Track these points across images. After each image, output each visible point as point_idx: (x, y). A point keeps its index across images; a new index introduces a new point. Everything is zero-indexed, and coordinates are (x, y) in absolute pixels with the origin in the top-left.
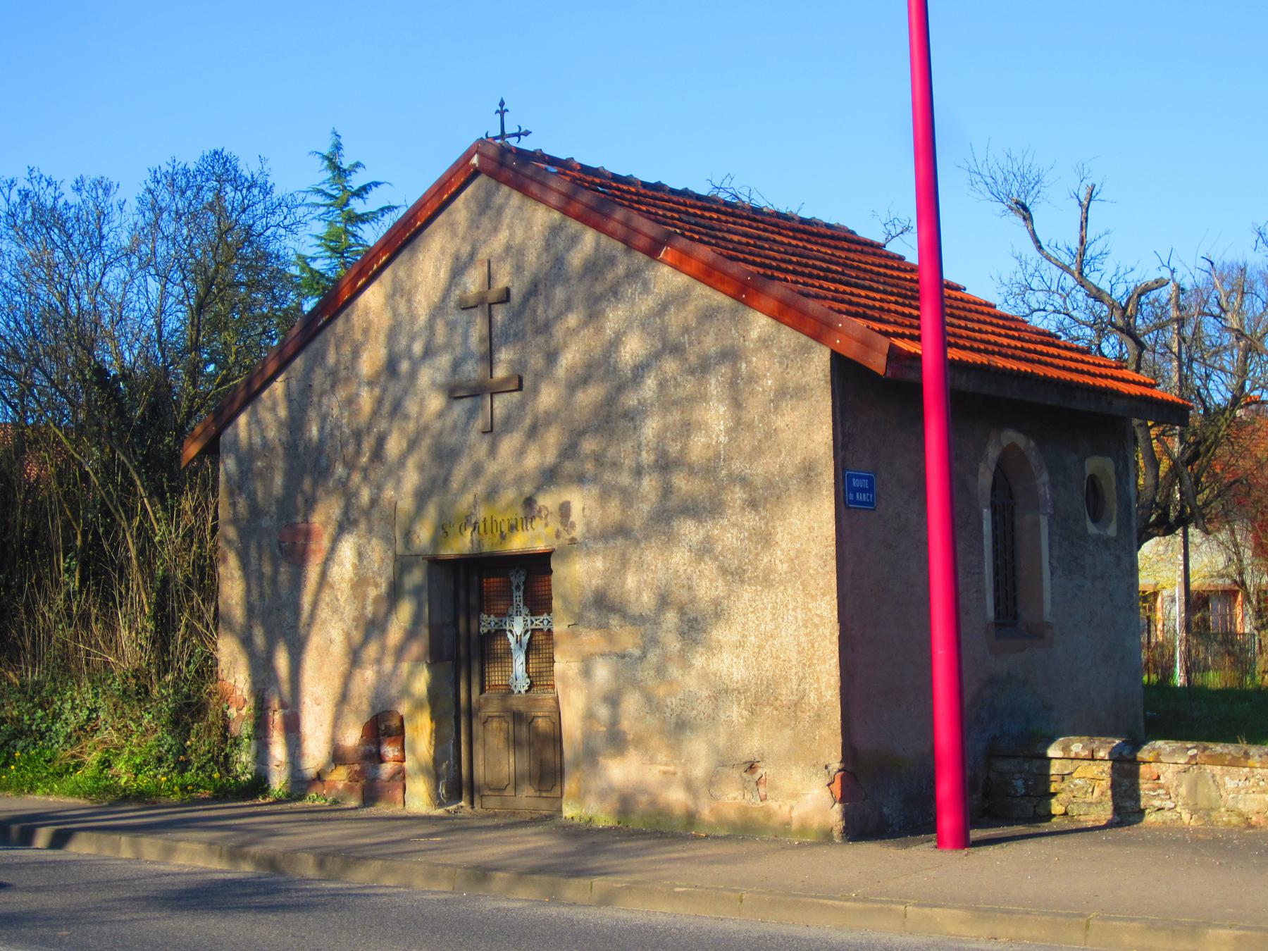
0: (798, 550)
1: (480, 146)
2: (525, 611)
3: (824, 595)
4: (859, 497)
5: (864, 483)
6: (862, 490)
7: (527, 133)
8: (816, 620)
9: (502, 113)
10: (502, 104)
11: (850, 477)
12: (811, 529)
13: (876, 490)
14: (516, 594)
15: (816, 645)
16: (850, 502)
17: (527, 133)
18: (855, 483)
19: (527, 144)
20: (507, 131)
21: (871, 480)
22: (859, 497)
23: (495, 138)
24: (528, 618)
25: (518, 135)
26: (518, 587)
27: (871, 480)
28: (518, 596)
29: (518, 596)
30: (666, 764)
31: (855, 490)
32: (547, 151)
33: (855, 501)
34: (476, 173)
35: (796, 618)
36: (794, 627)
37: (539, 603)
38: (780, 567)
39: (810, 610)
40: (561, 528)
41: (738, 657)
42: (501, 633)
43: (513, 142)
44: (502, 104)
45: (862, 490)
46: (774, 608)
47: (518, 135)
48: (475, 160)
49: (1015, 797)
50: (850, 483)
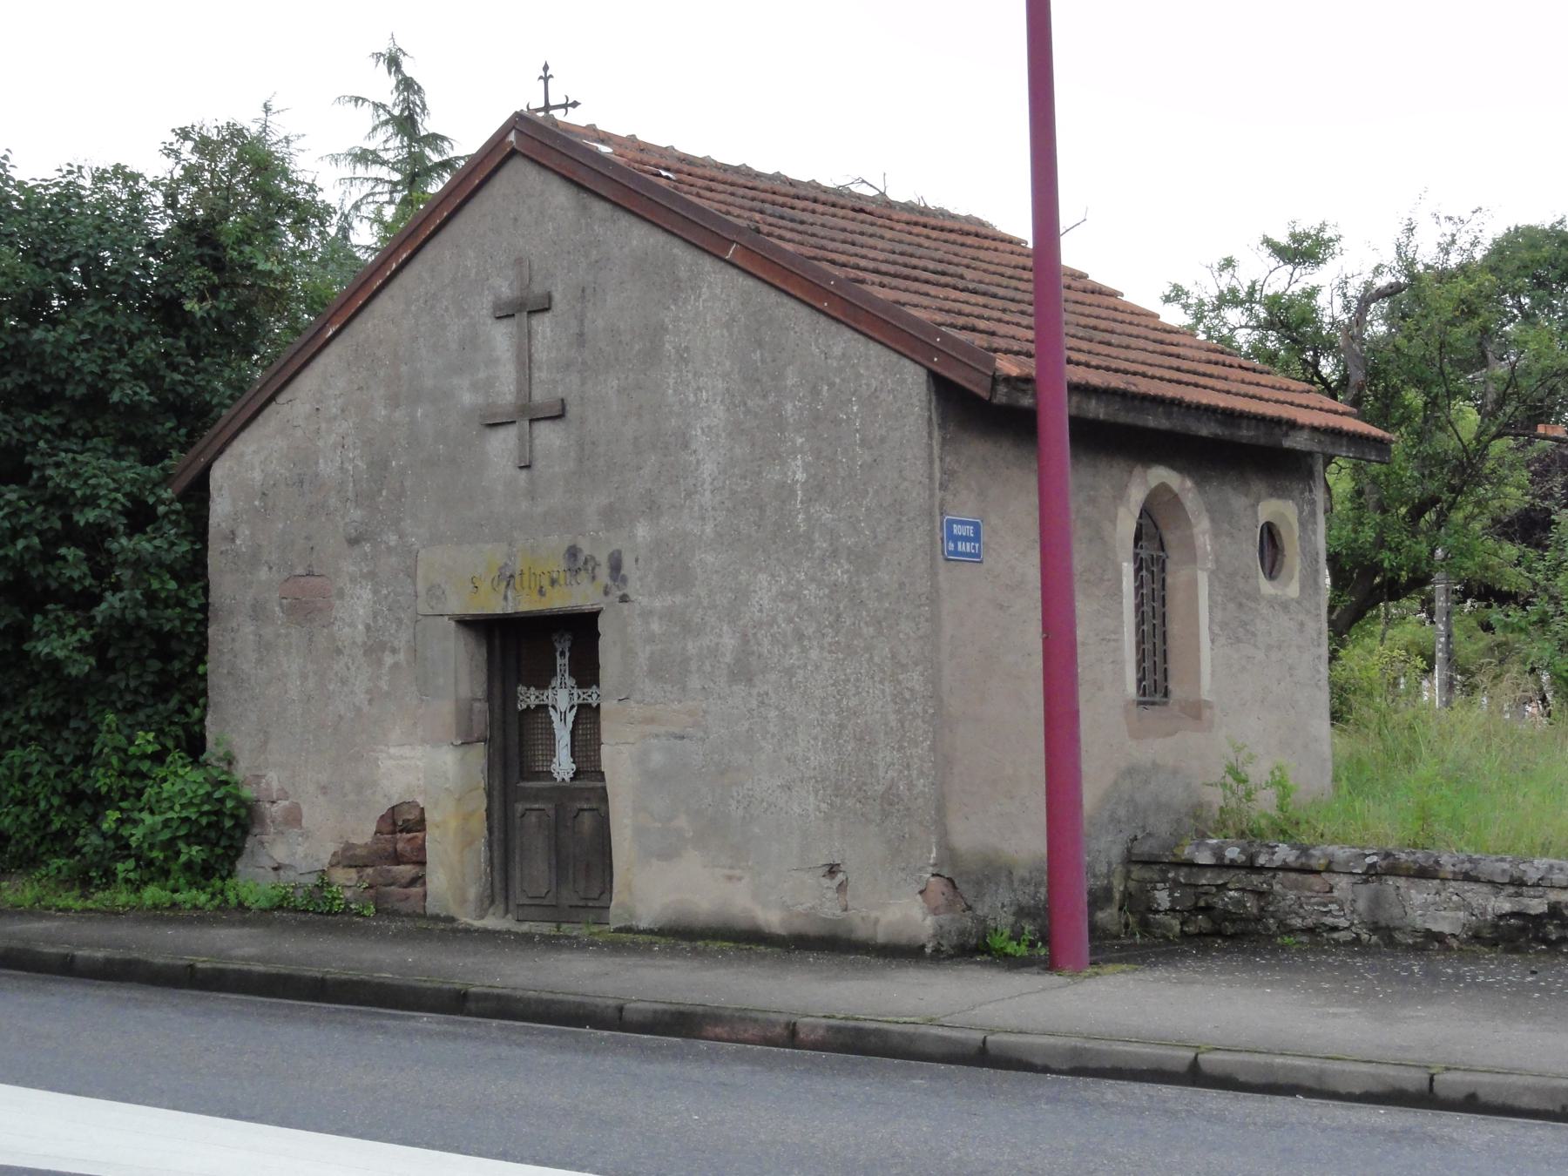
0: (886, 610)
1: (520, 122)
2: (570, 682)
3: (916, 664)
4: (961, 547)
5: (968, 531)
6: (966, 539)
7: (575, 104)
8: (907, 695)
9: (546, 79)
10: (546, 68)
11: (950, 523)
12: (902, 585)
13: (983, 538)
14: (559, 661)
15: (907, 724)
16: (950, 553)
17: (575, 104)
18: (957, 530)
19: (575, 118)
20: (552, 103)
21: (976, 526)
22: (961, 547)
23: (538, 110)
24: (575, 691)
25: (565, 106)
26: (563, 654)
27: (976, 526)
28: (562, 662)
29: (562, 662)
30: (731, 868)
31: (956, 539)
32: (602, 126)
33: (956, 553)
34: (513, 153)
35: (883, 691)
36: (880, 703)
37: (587, 671)
38: (865, 630)
39: (899, 682)
40: (610, 583)
41: (815, 738)
42: (543, 708)
43: (558, 115)
44: (546, 68)
45: (966, 539)
46: (858, 680)
47: (565, 106)
48: (512, 137)
49: (1157, 912)
50: (950, 529)
